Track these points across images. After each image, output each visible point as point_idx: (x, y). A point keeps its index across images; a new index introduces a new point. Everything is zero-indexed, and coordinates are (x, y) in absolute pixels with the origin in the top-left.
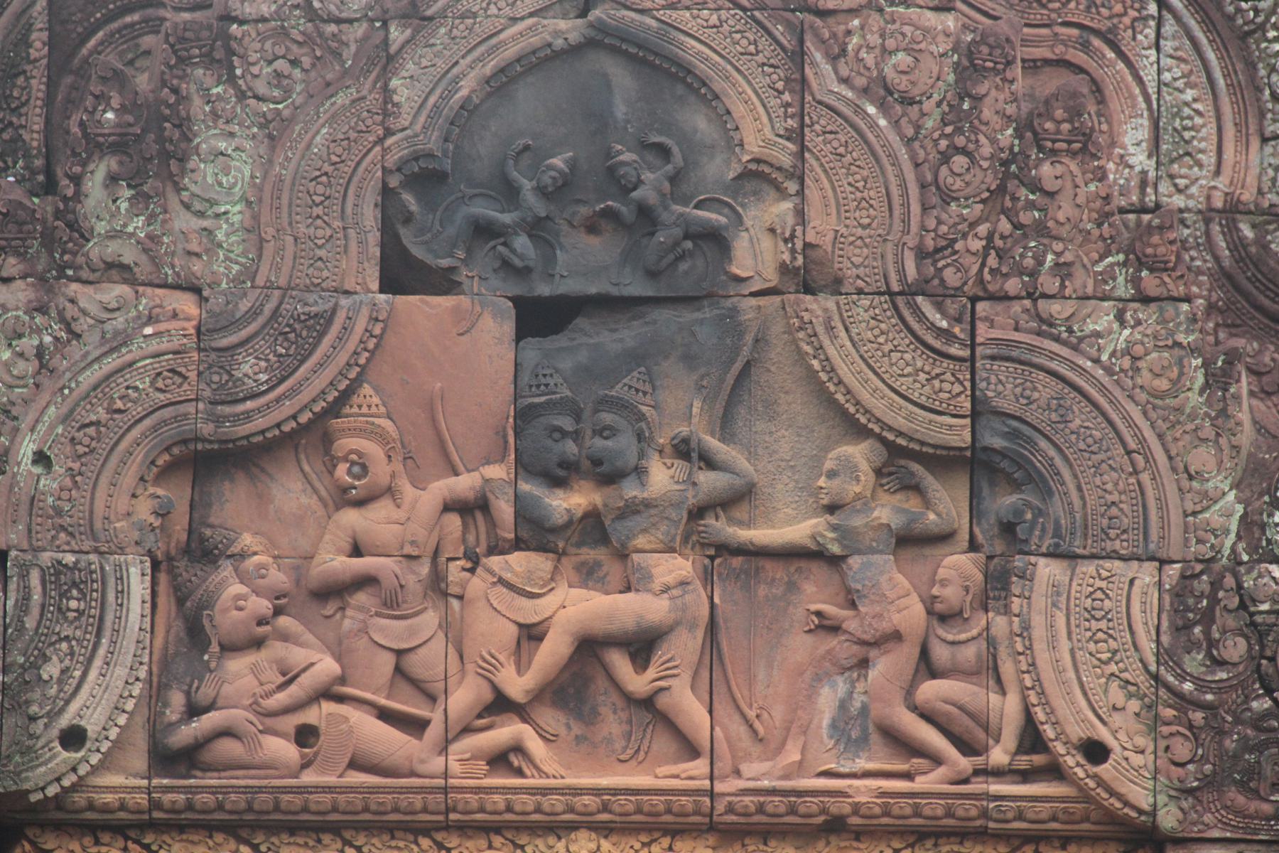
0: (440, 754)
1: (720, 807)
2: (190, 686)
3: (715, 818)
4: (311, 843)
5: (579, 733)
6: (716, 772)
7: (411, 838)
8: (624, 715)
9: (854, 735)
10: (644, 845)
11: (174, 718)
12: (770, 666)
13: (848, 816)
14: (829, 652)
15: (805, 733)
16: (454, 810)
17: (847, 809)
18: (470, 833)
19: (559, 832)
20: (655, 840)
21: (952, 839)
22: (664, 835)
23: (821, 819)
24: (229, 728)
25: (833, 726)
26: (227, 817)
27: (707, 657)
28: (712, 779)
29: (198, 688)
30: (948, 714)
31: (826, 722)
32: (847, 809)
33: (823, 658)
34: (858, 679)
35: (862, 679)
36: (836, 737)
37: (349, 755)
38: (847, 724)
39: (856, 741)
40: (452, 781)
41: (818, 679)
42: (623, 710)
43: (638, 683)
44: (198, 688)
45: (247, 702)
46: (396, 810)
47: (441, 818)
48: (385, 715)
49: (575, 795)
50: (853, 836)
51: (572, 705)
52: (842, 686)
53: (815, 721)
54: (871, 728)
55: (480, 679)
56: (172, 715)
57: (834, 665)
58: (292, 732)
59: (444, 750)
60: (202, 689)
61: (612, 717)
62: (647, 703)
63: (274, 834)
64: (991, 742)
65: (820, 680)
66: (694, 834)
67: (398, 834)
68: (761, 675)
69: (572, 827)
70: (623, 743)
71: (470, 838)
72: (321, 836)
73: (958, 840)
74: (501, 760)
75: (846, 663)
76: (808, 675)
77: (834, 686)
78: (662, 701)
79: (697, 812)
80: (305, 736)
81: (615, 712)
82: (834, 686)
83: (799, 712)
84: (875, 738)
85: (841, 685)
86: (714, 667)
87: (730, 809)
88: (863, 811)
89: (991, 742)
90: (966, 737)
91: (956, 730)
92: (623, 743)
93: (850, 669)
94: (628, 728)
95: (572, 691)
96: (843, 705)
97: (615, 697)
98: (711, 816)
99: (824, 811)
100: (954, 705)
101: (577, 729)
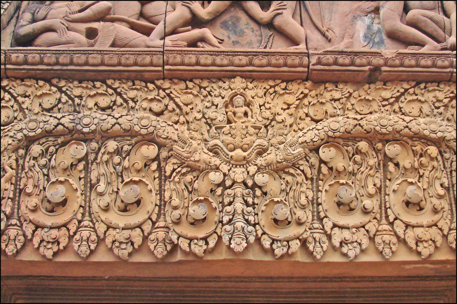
0: (161, 39)
1: (314, 60)
2: (35, 12)
3: (311, 67)
4: (90, 86)
5: (234, 40)
6: (309, 46)
7: (144, 84)
8: (258, 33)
9: (377, 40)
10: (271, 87)
11: (24, 23)
12: (331, 12)
13: (382, 66)
14: (359, 7)
15: (352, 38)
16: (167, 64)
17: (381, 62)
18: (176, 81)
19: (225, 80)
20: (277, 85)
21: (434, 84)
22: (283, 82)
23: (367, 68)
24: (51, 26)
25: (365, 36)
26: (45, 67)
27: (298, 12)
28: (307, 49)
29: (38, 12)
30: (425, 21)
31: (361, 34)
32: (381, 62)
33: (356, 9)
34: (374, 18)
35: (376, 19)
36: (368, 41)
37: (112, 39)
38: (372, 36)
39: (377, 43)
40: (165, 48)
41: (355, 18)
42: (257, 31)
43: (264, 15)
44: (38, 12)
45: (61, 16)
46: (136, 64)
47: (160, 68)
48: (133, 26)
49: (233, 56)
50: (383, 83)
51: (230, 29)
52: (367, 20)
53: (356, 36)
54: (384, 37)
55: (184, 7)
56: (22, 22)
57: (362, 12)
58: (84, 30)
59: (163, 38)
60: (40, 12)
61: (251, 34)
62: (270, 25)
63: (71, 83)
64: (447, 36)
65: (356, 18)
66: (299, 81)
67: (137, 82)
68: (327, 16)
69: (231, 76)
70: (258, 45)
71: (176, 84)
72: (95, 83)
73: (437, 84)
74: (193, 43)
75: (369, 10)
76: (350, 17)
77: (363, 21)
78: (278, 21)
79: (301, 65)
80: (91, 34)
81: (253, 31)
82: (363, 21)
83: (348, 30)
84: (387, 41)
85: (367, 20)
86: (302, 14)
87: (319, 63)
88: (390, 62)
89: (447, 36)
90: (435, 34)
91: (429, 30)
92: (258, 45)
93: (370, 12)
94: (260, 38)
95: (230, 23)
96: (369, 28)
97: (253, 25)
98: (308, 67)
99: (369, 64)
100: (427, 17)
101: (234, 38)
